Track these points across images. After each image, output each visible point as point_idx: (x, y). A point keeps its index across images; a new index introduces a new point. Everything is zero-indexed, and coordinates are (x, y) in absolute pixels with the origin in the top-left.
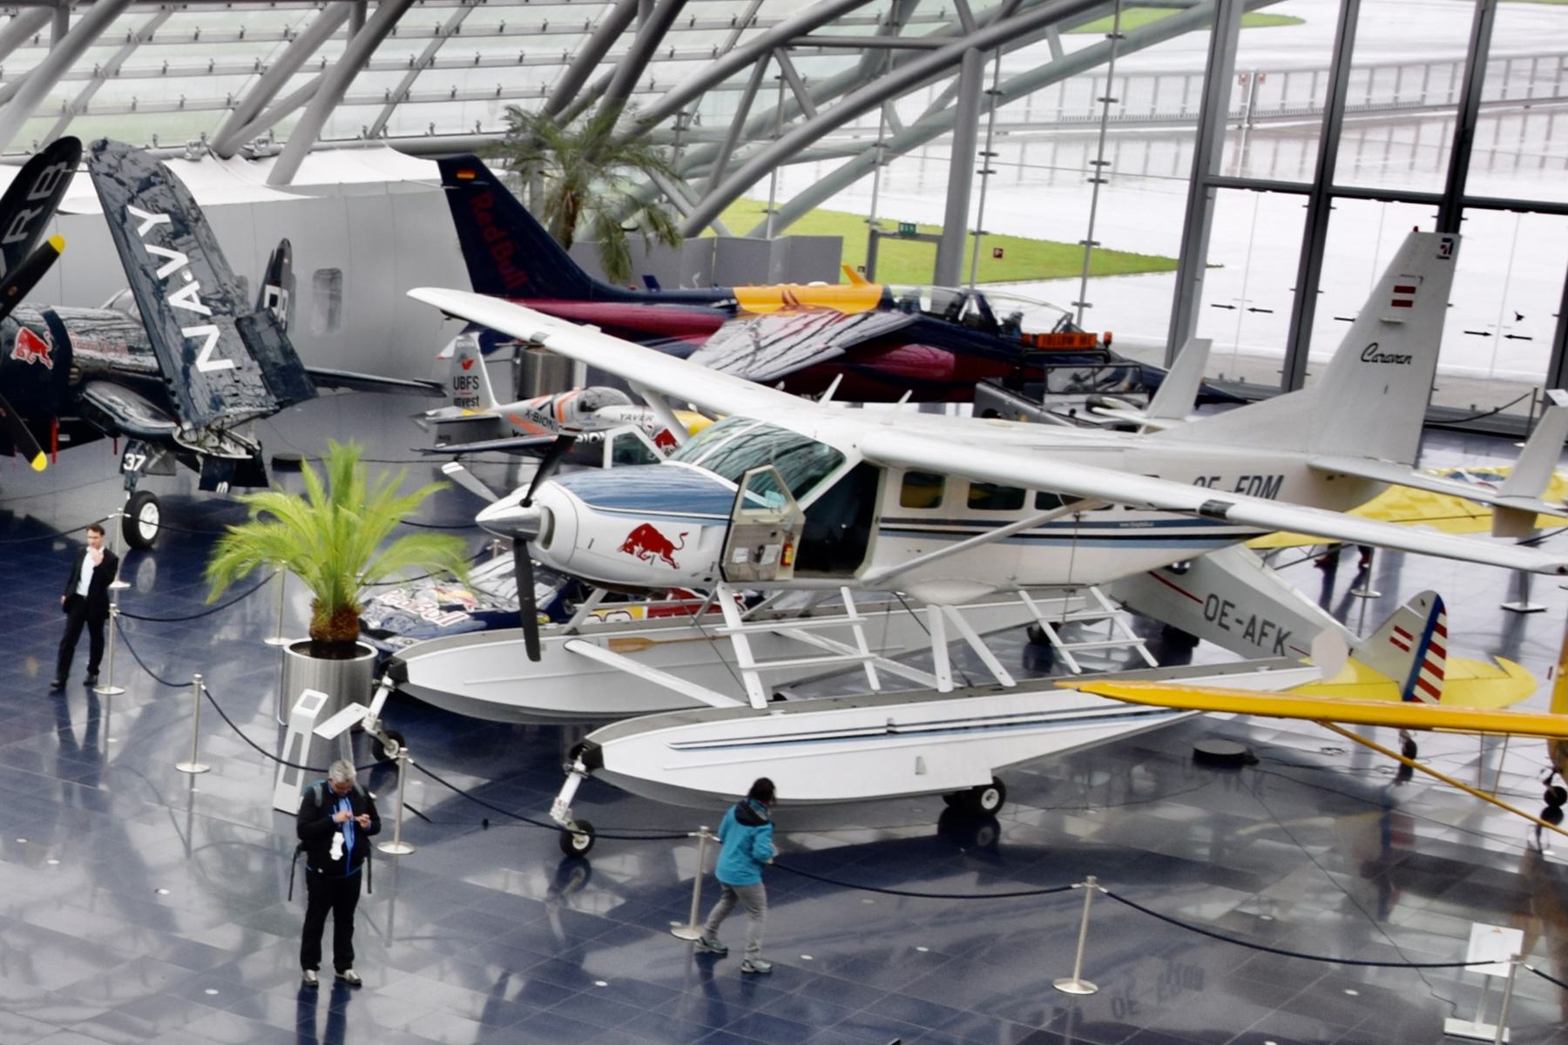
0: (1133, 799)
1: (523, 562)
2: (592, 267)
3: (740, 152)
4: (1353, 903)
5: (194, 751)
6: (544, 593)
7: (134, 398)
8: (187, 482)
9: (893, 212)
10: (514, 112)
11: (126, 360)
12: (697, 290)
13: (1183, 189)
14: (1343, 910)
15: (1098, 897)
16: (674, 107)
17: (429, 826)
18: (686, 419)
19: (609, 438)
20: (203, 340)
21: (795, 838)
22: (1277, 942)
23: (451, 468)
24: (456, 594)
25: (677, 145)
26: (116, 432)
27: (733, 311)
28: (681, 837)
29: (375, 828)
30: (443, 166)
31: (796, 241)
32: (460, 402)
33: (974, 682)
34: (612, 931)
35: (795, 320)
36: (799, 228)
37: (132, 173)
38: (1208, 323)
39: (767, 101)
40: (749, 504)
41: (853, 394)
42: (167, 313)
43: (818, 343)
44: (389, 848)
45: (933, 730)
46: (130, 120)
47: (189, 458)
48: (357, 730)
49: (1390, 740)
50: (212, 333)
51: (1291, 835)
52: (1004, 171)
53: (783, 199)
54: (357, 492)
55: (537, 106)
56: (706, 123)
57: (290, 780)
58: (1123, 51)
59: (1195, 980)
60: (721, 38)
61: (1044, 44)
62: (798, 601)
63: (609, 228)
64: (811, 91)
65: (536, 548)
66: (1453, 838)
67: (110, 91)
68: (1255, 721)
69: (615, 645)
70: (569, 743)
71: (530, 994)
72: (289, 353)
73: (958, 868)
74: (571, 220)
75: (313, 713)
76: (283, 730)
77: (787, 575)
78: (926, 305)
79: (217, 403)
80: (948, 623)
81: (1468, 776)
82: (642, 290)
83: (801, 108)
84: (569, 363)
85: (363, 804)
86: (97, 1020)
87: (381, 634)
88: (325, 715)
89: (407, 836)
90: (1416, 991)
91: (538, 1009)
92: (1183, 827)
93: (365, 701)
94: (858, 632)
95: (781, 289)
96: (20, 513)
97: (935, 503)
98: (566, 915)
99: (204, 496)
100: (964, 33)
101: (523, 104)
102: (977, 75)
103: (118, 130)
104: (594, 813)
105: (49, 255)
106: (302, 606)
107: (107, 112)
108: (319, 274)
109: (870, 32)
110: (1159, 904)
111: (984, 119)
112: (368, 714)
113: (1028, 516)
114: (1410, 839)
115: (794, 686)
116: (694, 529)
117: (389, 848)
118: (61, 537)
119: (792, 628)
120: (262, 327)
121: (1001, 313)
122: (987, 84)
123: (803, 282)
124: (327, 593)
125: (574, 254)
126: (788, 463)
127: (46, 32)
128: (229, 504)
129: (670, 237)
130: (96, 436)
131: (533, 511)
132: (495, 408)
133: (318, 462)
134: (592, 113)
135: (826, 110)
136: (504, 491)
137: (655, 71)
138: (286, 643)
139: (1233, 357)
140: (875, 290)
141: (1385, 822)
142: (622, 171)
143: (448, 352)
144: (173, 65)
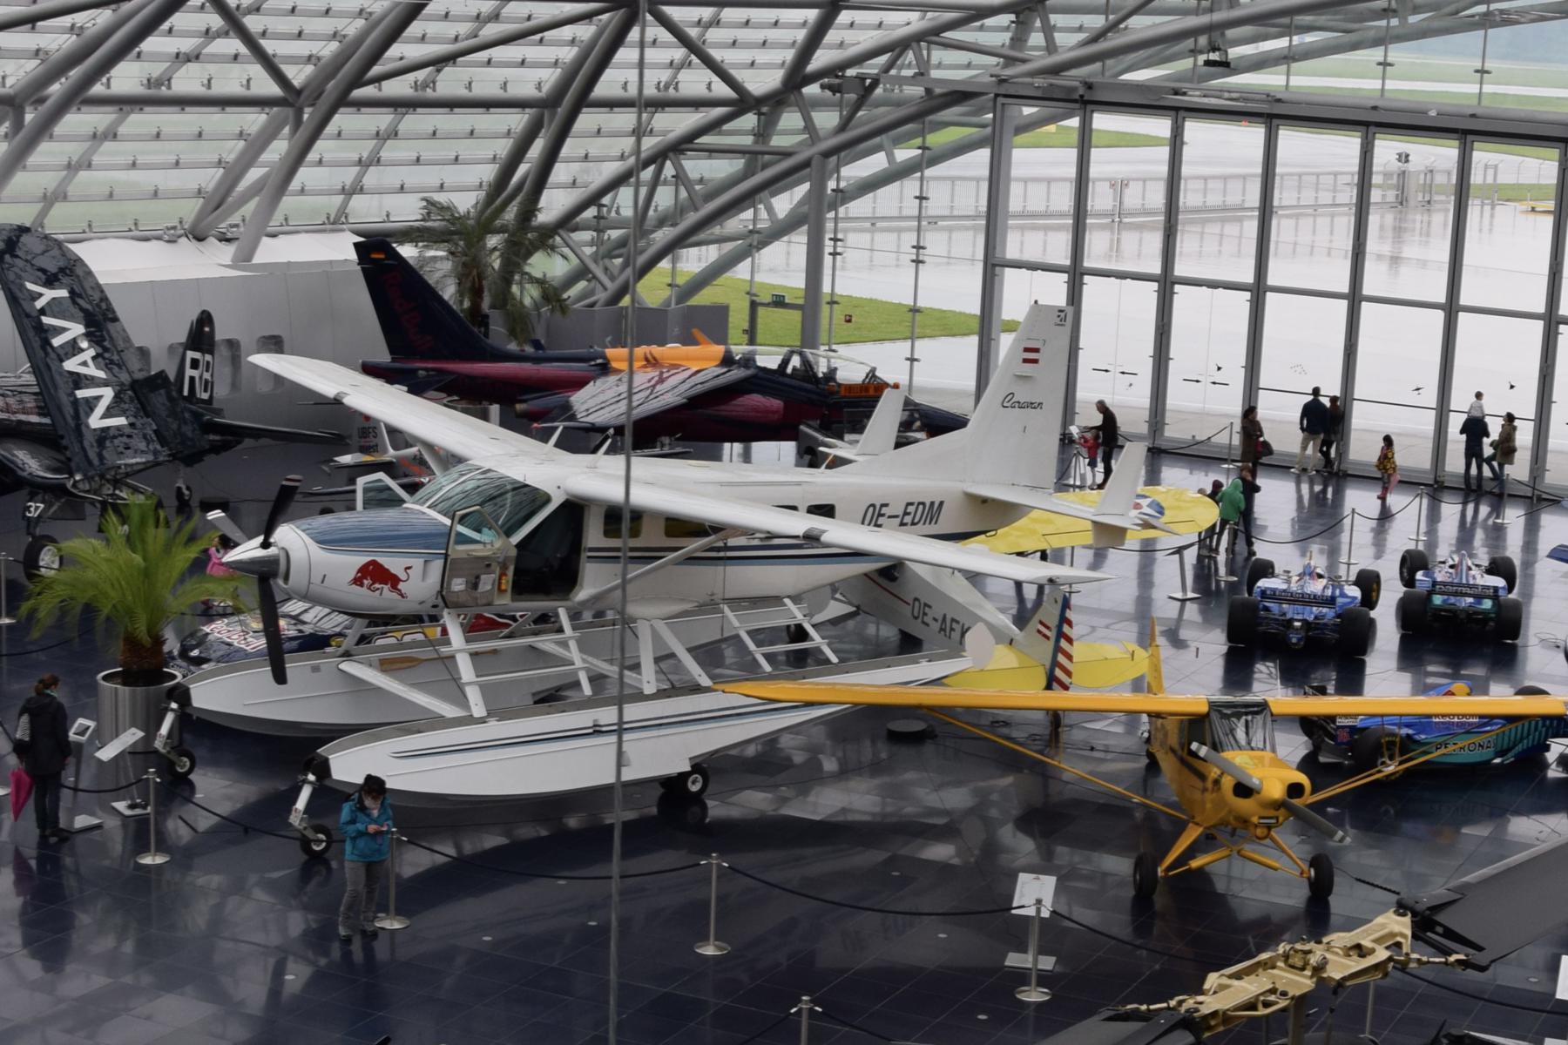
13: (979, 267)
123: (662, 344)
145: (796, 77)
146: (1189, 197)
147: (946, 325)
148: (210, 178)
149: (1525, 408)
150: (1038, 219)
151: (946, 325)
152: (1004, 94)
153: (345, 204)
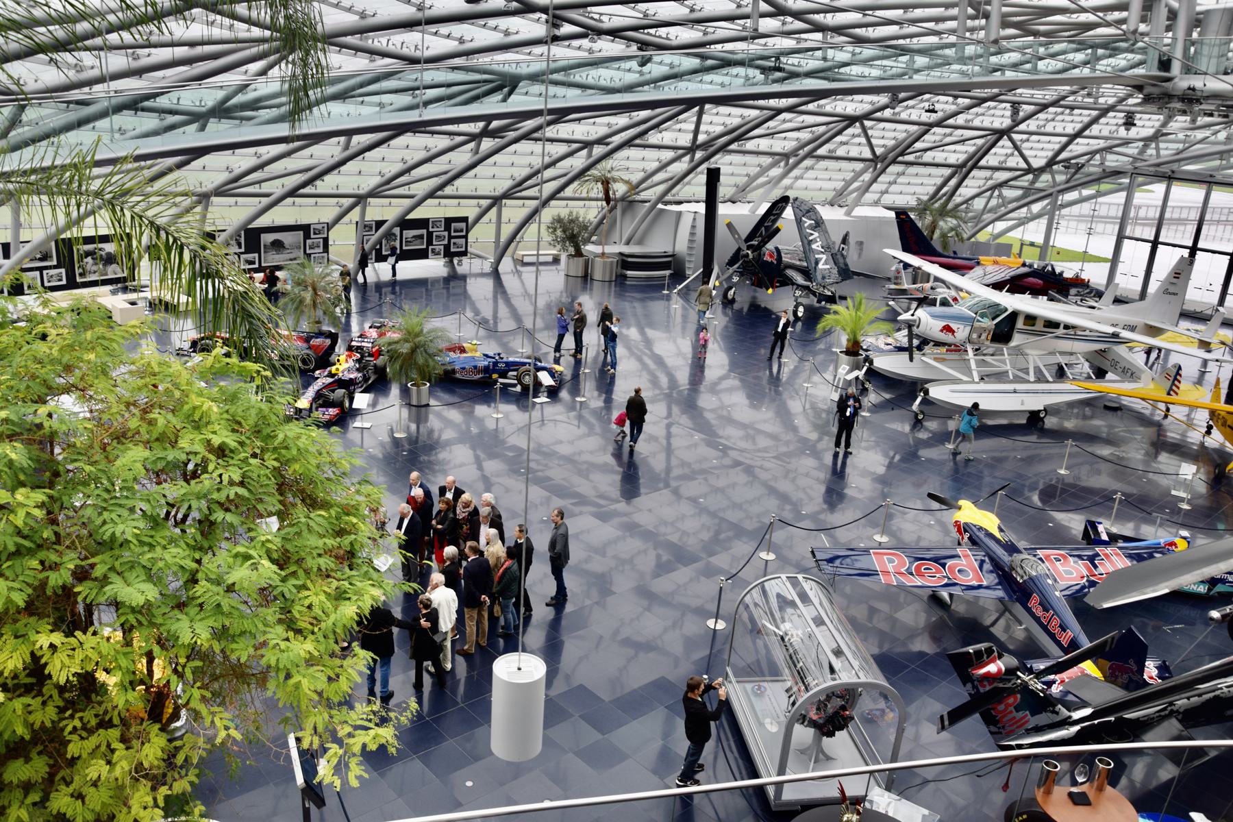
0: (1085, 417)
2: (939, 248)
3: (985, 217)
4: (1147, 454)
5: (808, 380)
6: (916, 342)
7: (799, 274)
8: (813, 301)
9: (1028, 238)
10: (919, 199)
11: (798, 263)
12: (969, 256)
13: (1115, 238)
14: (1145, 455)
15: (1072, 446)
16: (966, 202)
17: (876, 408)
18: (962, 294)
19: (939, 298)
20: (821, 259)
21: (984, 421)
22: (1124, 463)
23: (891, 303)
24: (890, 340)
25: (966, 213)
26: (793, 284)
27: (978, 263)
28: (950, 418)
29: (860, 407)
30: (896, 213)
31: (999, 244)
32: (895, 284)
33: (1040, 379)
34: (927, 444)
35: (996, 268)
36: (999, 241)
37: (804, 208)
38: (1118, 279)
39: (994, 202)
40: (978, 321)
42: (811, 250)
43: (1003, 275)
44: (864, 414)
45: (1027, 392)
46: (805, 192)
47: (814, 294)
48: (857, 378)
49: (1162, 406)
50: (824, 257)
51: (1130, 432)
52: (1062, 229)
53: (996, 231)
54: (863, 308)
55: (925, 198)
56: (975, 207)
57: (836, 391)
58: (1100, 196)
59: (1099, 472)
60: (981, 182)
62: (990, 351)
63: (944, 236)
64: (1007, 200)
65: (915, 328)
66: (1178, 437)
68: (1122, 397)
69: (936, 359)
72: (846, 265)
73: (1032, 434)
74: (933, 232)
76: (835, 376)
77: (988, 343)
78: (1036, 266)
79: (824, 278)
80: (1034, 360)
81: (1185, 419)
83: (1003, 205)
84: (929, 275)
85: (857, 400)
86: (773, 457)
87: (867, 350)
88: (848, 373)
89: (869, 411)
90: (1164, 481)
92: (1099, 427)
93: (860, 370)
94: (1008, 361)
95: (993, 258)
96: (763, 306)
97: (1033, 325)
98: (914, 438)
99: (818, 305)
100: (1054, 187)
101: (921, 197)
102: (1057, 200)
103: (802, 195)
104: (925, 408)
105: (778, 230)
106: (844, 340)
109: (1026, 184)
110: (1089, 449)
111: (1057, 213)
112: (861, 374)
113: (1061, 331)
114: (1166, 436)
115: (987, 376)
117: (864, 414)
118: (774, 314)
119: (988, 359)
120: (839, 256)
121: (1058, 270)
122: (1059, 203)
124: (852, 337)
125: (933, 243)
126: (991, 310)
127: (782, 164)
128: (825, 308)
129: (962, 240)
130: (788, 285)
131: (914, 317)
132: (906, 286)
133: (852, 298)
134: (942, 201)
135: (1011, 206)
136: (906, 311)
137: (961, 190)
138: (838, 351)
139: (1125, 289)
140: (1021, 261)
141: (1158, 431)
142: (949, 219)
143: (893, 268)
144: (819, 177)
146: (1208, 217)
148: (839, 185)
150: (1145, 222)
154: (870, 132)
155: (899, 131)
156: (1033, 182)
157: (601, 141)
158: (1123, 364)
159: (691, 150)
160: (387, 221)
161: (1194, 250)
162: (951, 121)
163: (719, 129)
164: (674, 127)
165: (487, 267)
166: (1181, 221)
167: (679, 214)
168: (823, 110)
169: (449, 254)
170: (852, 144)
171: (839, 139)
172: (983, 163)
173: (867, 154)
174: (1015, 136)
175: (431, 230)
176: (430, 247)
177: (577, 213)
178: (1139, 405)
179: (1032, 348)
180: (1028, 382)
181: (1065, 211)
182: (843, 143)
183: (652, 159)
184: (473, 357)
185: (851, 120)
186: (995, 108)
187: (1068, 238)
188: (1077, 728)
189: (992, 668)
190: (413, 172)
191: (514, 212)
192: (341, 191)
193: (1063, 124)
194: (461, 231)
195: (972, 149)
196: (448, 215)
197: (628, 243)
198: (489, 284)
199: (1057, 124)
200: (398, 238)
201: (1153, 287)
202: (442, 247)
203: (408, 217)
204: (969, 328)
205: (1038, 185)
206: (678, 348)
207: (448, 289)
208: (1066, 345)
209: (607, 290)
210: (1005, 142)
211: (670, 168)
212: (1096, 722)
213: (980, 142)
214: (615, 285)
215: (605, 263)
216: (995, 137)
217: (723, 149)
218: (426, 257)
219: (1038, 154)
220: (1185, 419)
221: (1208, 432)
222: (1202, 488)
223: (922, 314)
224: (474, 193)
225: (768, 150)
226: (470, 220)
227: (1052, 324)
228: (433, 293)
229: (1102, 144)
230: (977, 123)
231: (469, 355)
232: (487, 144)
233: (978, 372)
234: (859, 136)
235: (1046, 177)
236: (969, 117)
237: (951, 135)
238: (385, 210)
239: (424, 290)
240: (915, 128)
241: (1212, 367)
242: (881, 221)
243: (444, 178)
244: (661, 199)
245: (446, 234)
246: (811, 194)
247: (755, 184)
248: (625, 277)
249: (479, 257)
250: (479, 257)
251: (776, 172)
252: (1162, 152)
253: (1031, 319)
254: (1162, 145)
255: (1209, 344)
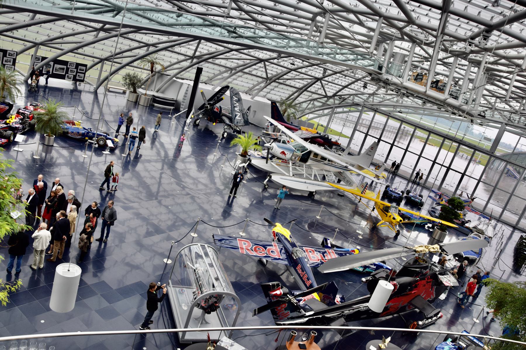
0: (330, 197)
1: (268, 152)
2: (286, 119)
3: (306, 111)
4: (351, 215)
5: (224, 164)
6: (270, 156)
8: (231, 131)
9: (321, 123)
10: (281, 98)
11: (228, 114)
12: (297, 125)
13: (353, 129)
15: (323, 208)
16: (300, 103)
17: (249, 180)
21: (292, 192)
23: (263, 138)
24: (260, 153)
25: (299, 108)
26: (224, 123)
27: (300, 129)
28: (278, 189)
29: (243, 179)
31: (309, 123)
32: (266, 131)
35: (307, 132)
36: (310, 122)
37: (235, 92)
38: (352, 146)
39: (310, 106)
40: (296, 152)
41: (311, 142)
42: (234, 110)
43: (309, 135)
44: (244, 182)
47: (232, 128)
48: (244, 166)
49: (359, 198)
50: (239, 114)
51: (346, 206)
52: (334, 122)
53: (309, 118)
54: (251, 138)
55: (284, 99)
57: (234, 170)
59: (332, 220)
60: (307, 97)
61: (342, 109)
63: (289, 115)
64: (316, 106)
65: (270, 150)
66: (363, 210)
67: (235, 82)
69: (276, 164)
70: (268, 174)
71: (256, 203)
72: (248, 119)
73: (308, 200)
74: (285, 113)
75: (239, 163)
76: (235, 164)
77: (298, 161)
78: (322, 135)
79: (237, 123)
82: (291, 124)
83: (314, 108)
85: (242, 175)
87: (249, 156)
88: (240, 164)
89: (246, 181)
90: (355, 226)
91: (257, 205)
93: (246, 163)
94: (304, 170)
96: (210, 129)
97: (317, 157)
98: (263, 195)
99: (233, 133)
100: (334, 105)
101: (283, 98)
104: (269, 183)
105: (222, 99)
106: (241, 150)
107: (234, 84)
108: (254, 111)
109: (324, 101)
110: (330, 210)
112: (245, 165)
113: (327, 162)
114: (358, 209)
116: (289, 153)
117: (244, 182)
118: (214, 134)
119: (297, 168)
120: (245, 115)
121: (330, 138)
124: (244, 149)
125: (284, 117)
127: (229, 72)
128: (236, 135)
129: (295, 118)
130: (222, 123)
132: (270, 133)
133: (247, 133)
134: (290, 101)
135: (317, 109)
136: (268, 143)
137: (299, 98)
138: (238, 154)
140: (317, 131)
142: (292, 109)
143: (266, 124)
145: (335, 95)
146: (386, 128)
147: (345, 137)
148: (251, 86)
149: (426, 173)
151: (345, 137)
152: (364, 106)
153: (267, 94)
154: (267, 67)
155: (279, 69)
156: (327, 101)
157: (154, 45)
158: (347, 179)
159: (192, 58)
160: (47, 58)
161: (379, 140)
162: (300, 70)
163: (206, 52)
164: (187, 46)
165: (92, 89)
166: (377, 128)
167: (182, 84)
168: (250, 54)
169: (75, 79)
170: (259, 70)
171: (254, 67)
172: (309, 89)
173: (264, 76)
174: (323, 82)
175: (68, 67)
176: (67, 75)
177: (138, 74)
178: (350, 196)
179: (315, 167)
180: (311, 180)
181: (336, 115)
182: (255, 69)
183: (174, 58)
184: (78, 128)
185: (261, 61)
186: (317, 69)
187: (335, 126)
188: (307, 319)
189: (278, 292)
190: (64, 39)
191: (108, 67)
192: (26, 39)
193: (342, 81)
194: (83, 70)
195: (306, 83)
196: (78, 62)
197: (157, 91)
198: (92, 97)
199: (340, 81)
200: (52, 67)
201: (363, 151)
202: (72, 76)
203: (58, 59)
204: (292, 154)
205: (328, 103)
206: (171, 141)
207: (72, 95)
208: (328, 168)
209: (144, 110)
210: (319, 83)
211: (181, 63)
212: (314, 317)
213: (309, 81)
214: (149, 109)
215: (146, 98)
216: (316, 80)
217: (206, 60)
218: (64, 79)
219: (331, 90)
220: (366, 204)
221: (373, 210)
222: (368, 231)
223: (274, 145)
224: (92, 55)
225: (224, 65)
226: (88, 67)
227: (324, 158)
228: (64, 95)
229: (354, 92)
230: (309, 73)
231: (76, 126)
232: (102, 34)
233: (292, 172)
234: (262, 68)
235: (331, 100)
236: (307, 70)
237: (298, 75)
238: (48, 53)
239: (60, 93)
240: (285, 69)
241: (379, 185)
242: (265, 104)
243: (79, 45)
244: (175, 76)
245: (75, 70)
246: (239, 87)
247: (216, 78)
248: (154, 106)
249: (89, 84)
250: (89, 84)
251: (226, 75)
252: (375, 101)
253: (316, 155)
254: (375, 98)
255: (379, 176)
